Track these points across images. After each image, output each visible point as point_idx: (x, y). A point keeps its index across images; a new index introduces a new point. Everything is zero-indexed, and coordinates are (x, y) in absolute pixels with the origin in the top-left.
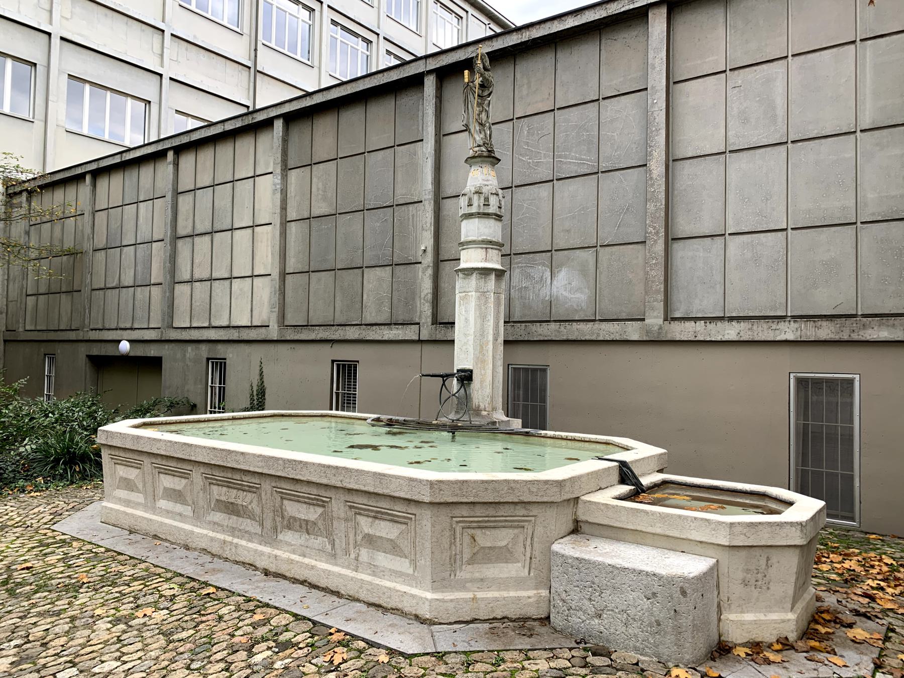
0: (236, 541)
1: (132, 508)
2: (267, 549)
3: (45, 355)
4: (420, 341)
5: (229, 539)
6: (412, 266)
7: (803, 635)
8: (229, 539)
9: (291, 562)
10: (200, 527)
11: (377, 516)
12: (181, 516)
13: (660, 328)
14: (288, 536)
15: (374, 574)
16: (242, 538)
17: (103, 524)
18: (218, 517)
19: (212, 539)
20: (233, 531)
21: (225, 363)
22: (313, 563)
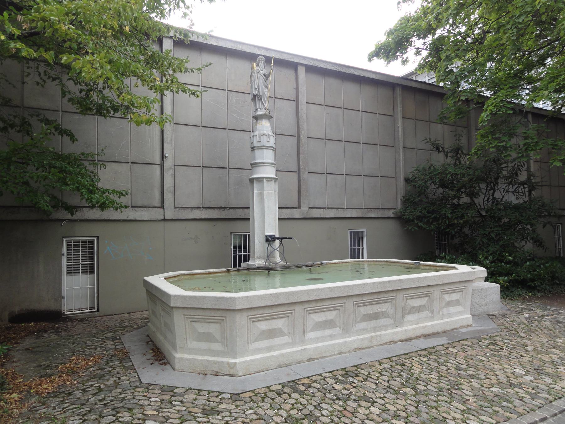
0: (378, 333)
1: (277, 350)
2: (399, 329)
3: (231, 233)
4: (164, 220)
5: (373, 334)
6: (150, 166)
7: (156, 347)
8: (373, 334)
9: (414, 329)
10: (349, 337)
11: (452, 292)
12: (332, 337)
13: (307, 212)
14: (410, 317)
15: (450, 317)
16: (381, 330)
17: (257, 374)
18: (363, 325)
19: (362, 340)
20: (375, 329)
21: (249, 235)
22: (425, 325)
